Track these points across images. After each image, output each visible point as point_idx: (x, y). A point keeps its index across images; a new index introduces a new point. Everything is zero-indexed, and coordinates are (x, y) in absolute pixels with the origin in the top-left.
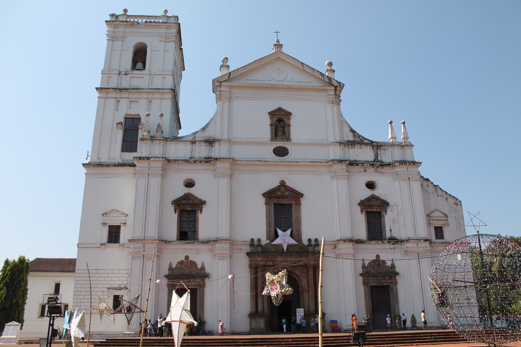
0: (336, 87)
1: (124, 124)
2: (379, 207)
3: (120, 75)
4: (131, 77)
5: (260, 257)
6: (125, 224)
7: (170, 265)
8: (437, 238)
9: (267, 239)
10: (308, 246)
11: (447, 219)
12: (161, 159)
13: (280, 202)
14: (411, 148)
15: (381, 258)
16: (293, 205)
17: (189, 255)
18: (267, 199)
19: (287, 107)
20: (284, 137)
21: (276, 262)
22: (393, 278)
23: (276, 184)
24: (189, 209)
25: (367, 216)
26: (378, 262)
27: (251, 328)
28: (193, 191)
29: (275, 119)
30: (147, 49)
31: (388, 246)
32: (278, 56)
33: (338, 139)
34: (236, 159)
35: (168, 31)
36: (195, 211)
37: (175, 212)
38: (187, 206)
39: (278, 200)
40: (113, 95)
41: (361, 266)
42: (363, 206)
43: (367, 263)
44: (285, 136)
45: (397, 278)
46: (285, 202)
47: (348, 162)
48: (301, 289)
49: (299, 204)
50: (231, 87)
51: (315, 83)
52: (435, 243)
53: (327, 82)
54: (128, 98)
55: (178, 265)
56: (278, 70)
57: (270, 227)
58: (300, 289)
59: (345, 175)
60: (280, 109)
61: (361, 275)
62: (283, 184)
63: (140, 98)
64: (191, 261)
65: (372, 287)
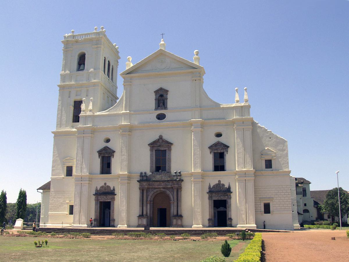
9: (150, 172)
15: (221, 183)
16: (167, 151)
19: (165, 87)
21: (154, 186)
22: (228, 195)
23: (157, 137)
24: (107, 155)
27: (138, 224)
28: (109, 145)
36: (110, 157)
37: (99, 158)
38: (106, 154)
41: (208, 187)
42: (211, 149)
43: (212, 186)
44: (164, 106)
49: (170, 150)
55: (101, 189)
57: (152, 164)
60: (161, 89)
62: (161, 137)
64: (107, 186)
65: (214, 201)
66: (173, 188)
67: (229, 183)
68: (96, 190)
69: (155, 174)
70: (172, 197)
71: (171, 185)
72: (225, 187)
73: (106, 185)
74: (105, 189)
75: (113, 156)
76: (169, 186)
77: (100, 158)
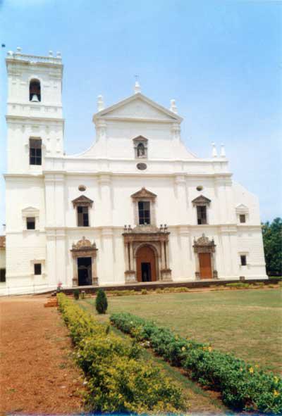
16: (151, 203)
23: (139, 189)
26: (203, 238)
29: (137, 144)
49: (154, 202)
50: (106, 120)
51: (165, 119)
60: (141, 137)
62: (144, 189)
70: (158, 251)
74: (84, 244)
75: (91, 207)
76: (156, 240)
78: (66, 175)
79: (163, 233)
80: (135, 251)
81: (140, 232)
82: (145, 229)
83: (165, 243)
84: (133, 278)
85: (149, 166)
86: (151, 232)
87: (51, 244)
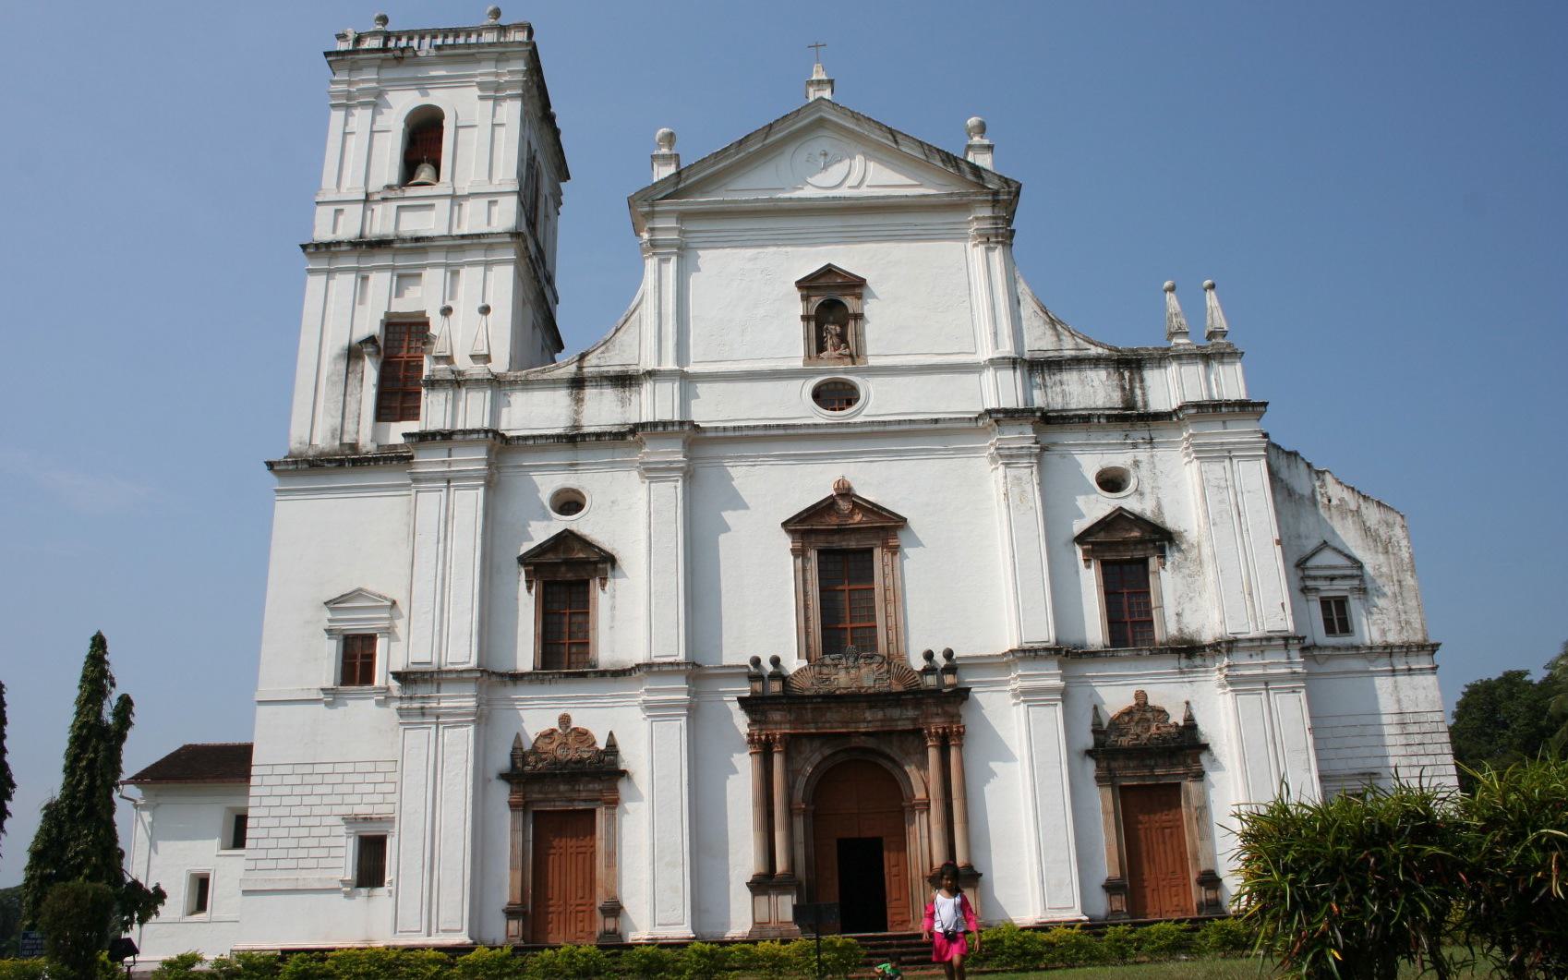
0: (996, 193)
1: (381, 344)
2: (1140, 547)
3: (368, 204)
4: (398, 207)
5: (778, 710)
6: (389, 632)
7: (515, 742)
8: (1330, 630)
10: (926, 671)
11: (1359, 573)
12: (482, 436)
13: (836, 545)
14: (1233, 360)
15: (1151, 702)
16: (877, 553)
17: (569, 712)
18: (797, 536)
20: (843, 352)
22: (1189, 761)
24: (570, 576)
25: (1104, 574)
29: (816, 301)
30: (444, 124)
31: (1169, 664)
32: (817, 115)
33: (1007, 349)
34: (701, 425)
35: (504, 69)
36: (586, 583)
37: (529, 589)
38: (563, 569)
39: (830, 538)
40: (351, 263)
44: (848, 347)
45: (1204, 758)
46: (853, 545)
47: (1038, 414)
48: (907, 804)
50: (683, 216)
52: (1326, 647)
53: (971, 181)
54: (393, 268)
56: (821, 154)
58: (903, 804)
59: (1030, 456)
60: (829, 270)
61: (1089, 753)
62: (845, 492)
63: (424, 267)
64: (575, 729)
66: (921, 730)
67: (1187, 703)
68: (514, 749)
69: (827, 666)
71: (914, 720)
72: (1171, 721)
73: (568, 727)
74: (564, 745)
75: (604, 581)
76: (901, 725)
77: (533, 591)
78: (500, 445)
79: (935, 694)
80: (801, 783)
81: (824, 689)
82: (843, 679)
83: (950, 739)
84: (785, 906)
85: (867, 386)
86: (882, 687)
87: (419, 739)
